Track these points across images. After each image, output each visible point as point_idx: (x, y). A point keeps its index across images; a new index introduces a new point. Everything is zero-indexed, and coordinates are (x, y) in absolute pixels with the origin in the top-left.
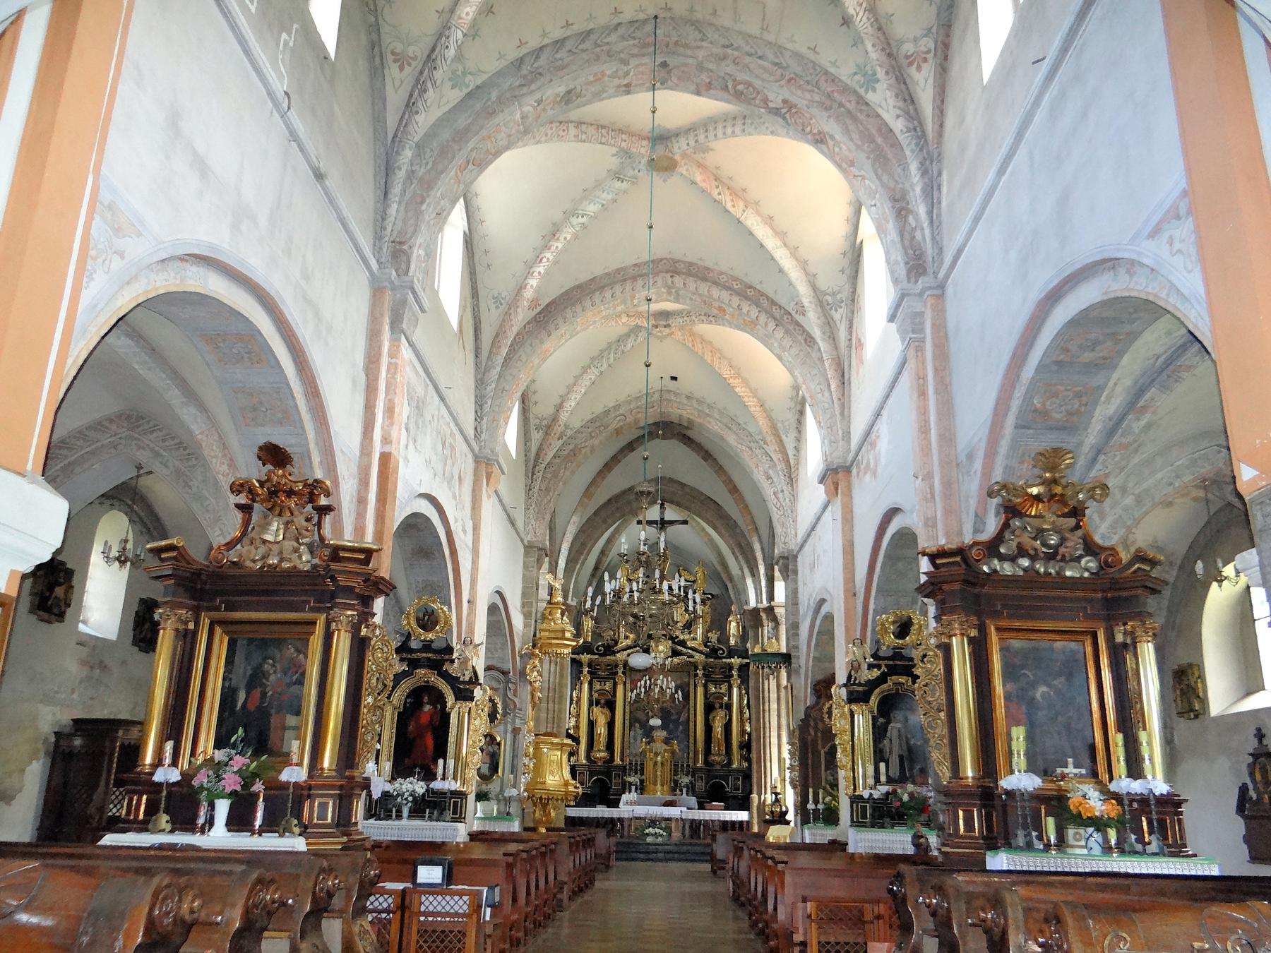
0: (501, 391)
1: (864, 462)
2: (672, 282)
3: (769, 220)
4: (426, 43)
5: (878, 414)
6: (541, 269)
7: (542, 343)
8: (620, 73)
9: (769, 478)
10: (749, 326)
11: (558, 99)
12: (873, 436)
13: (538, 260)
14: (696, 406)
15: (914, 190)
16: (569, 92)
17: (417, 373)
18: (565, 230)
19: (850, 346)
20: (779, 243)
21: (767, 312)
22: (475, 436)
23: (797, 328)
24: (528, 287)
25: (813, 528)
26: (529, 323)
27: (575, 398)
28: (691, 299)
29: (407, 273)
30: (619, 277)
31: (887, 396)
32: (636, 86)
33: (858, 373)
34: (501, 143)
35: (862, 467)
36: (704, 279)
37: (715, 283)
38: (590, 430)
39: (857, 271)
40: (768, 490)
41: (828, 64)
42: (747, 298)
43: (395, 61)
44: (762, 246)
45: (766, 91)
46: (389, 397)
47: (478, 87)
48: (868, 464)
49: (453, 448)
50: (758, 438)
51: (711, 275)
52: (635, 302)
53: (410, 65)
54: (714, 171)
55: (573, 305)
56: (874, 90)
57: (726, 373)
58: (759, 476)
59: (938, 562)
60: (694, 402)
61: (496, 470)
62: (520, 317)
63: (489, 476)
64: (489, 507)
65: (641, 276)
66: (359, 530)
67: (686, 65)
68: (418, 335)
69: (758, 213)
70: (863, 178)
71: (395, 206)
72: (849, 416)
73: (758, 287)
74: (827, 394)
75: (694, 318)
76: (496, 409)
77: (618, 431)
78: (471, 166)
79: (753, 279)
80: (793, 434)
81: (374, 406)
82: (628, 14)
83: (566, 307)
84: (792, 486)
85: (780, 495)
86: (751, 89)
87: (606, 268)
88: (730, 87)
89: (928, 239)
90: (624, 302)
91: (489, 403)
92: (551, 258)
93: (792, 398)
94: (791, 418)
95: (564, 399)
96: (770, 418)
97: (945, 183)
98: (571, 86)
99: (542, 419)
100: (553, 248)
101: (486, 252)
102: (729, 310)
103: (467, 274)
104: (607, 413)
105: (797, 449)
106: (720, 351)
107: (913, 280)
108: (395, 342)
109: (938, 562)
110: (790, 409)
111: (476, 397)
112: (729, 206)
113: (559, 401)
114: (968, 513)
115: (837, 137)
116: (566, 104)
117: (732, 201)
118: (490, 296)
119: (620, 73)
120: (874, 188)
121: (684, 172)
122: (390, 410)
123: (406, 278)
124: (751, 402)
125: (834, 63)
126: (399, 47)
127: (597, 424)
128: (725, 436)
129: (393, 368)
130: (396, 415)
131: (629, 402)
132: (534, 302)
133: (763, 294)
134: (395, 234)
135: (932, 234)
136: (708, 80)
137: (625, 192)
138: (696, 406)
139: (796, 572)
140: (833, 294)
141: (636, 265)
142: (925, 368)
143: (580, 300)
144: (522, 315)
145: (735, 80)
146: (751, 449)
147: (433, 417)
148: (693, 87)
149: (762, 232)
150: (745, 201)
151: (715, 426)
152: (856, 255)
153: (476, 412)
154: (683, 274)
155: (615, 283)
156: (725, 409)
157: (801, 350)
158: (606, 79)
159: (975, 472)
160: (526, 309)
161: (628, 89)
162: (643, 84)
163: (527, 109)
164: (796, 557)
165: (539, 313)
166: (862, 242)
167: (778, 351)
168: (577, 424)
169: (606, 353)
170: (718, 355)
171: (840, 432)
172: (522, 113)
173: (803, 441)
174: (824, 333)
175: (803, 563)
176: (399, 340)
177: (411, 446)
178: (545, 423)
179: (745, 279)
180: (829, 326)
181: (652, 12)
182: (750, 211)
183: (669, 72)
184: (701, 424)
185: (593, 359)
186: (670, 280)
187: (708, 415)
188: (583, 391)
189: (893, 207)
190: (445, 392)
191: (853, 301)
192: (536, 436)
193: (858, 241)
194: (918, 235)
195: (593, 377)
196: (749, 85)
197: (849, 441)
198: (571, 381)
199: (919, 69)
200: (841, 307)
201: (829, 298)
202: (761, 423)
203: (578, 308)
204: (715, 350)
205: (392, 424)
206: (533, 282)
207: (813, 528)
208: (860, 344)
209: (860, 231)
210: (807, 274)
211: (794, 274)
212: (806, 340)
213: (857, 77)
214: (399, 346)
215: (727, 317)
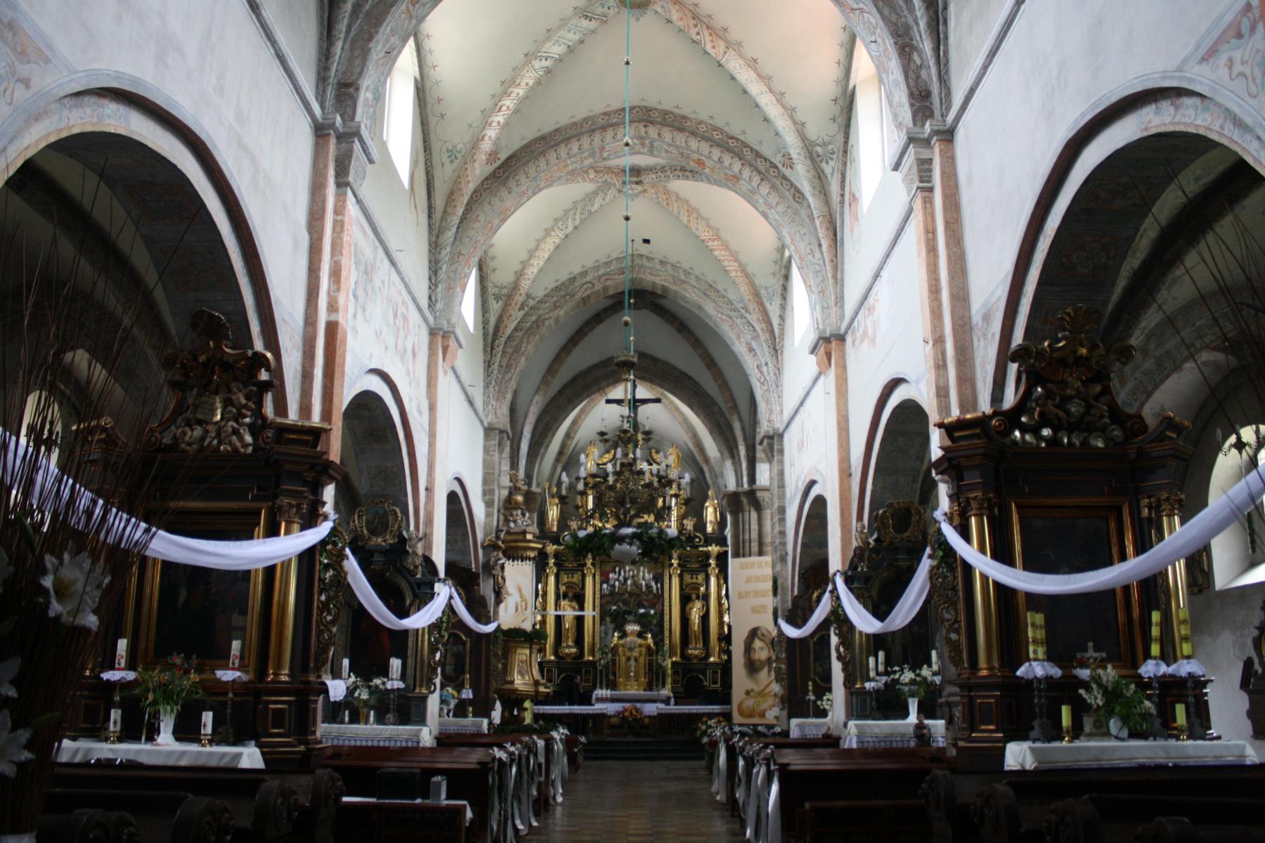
0: (456, 256)
1: (861, 330)
2: (646, 132)
3: (753, 63)
5: (877, 276)
6: (500, 118)
7: (501, 200)
9: (751, 350)
10: (731, 181)
12: (871, 300)
13: (495, 107)
14: (671, 272)
15: (917, 24)
17: (365, 233)
18: (528, 75)
19: (842, 202)
20: (764, 88)
21: (751, 165)
22: (430, 306)
23: (785, 182)
24: (486, 138)
25: (802, 404)
26: (487, 179)
27: (537, 263)
28: (667, 151)
29: (353, 118)
30: (586, 127)
31: (888, 256)
33: (852, 231)
35: (858, 335)
36: (681, 130)
37: (693, 134)
38: (554, 299)
39: (849, 119)
40: (750, 364)
42: (729, 150)
44: (745, 92)
46: (334, 259)
48: (865, 332)
49: (405, 319)
50: (739, 306)
51: (689, 124)
52: (605, 155)
54: (692, 8)
55: (536, 158)
57: (705, 235)
58: (740, 349)
59: (957, 434)
60: (669, 267)
61: (452, 344)
62: (477, 172)
63: (445, 349)
64: (446, 383)
65: (612, 125)
66: (305, 409)
68: (365, 190)
69: (741, 56)
70: (862, 11)
71: (340, 44)
72: (842, 280)
73: (741, 137)
74: (818, 255)
75: (669, 173)
76: (452, 275)
77: (585, 300)
79: (735, 130)
80: (778, 301)
81: (319, 269)
83: (528, 162)
84: (777, 358)
85: (764, 369)
87: (572, 117)
89: (935, 79)
90: (592, 155)
91: (444, 268)
92: (512, 106)
93: (776, 262)
94: (776, 284)
95: (525, 264)
96: (752, 284)
97: (953, 17)
99: (502, 287)
100: (513, 95)
101: (439, 100)
102: (709, 163)
103: (419, 123)
104: (572, 280)
105: (782, 318)
106: (697, 210)
107: (919, 123)
108: (341, 198)
109: (957, 434)
110: (774, 274)
111: (430, 262)
112: (709, 48)
113: (518, 267)
114: (985, 383)
117: (712, 41)
118: (444, 149)
120: (873, 21)
121: (659, 10)
122: (336, 274)
123: (352, 124)
124: (732, 266)
127: (562, 293)
128: (703, 305)
129: (339, 226)
130: (343, 279)
131: (597, 268)
132: (493, 155)
133: (746, 146)
134: (339, 74)
135: (940, 74)
137: (593, 32)
138: (671, 272)
139: (781, 452)
140: (824, 144)
141: (605, 114)
142: (933, 221)
143: (543, 153)
144: (479, 170)
146: (730, 317)
147: (383, 282)
149: (746, 77)
150: (726, 42)
151: (691, 295)
152: (848, 100)
153: (430, 279)
154: (658, 123)
155: (582, 134)
156: (703, 275)
157: (789, 207)
159: (993, 335)
160: (484, 162)
164: (781, 436)
165: (499, 168)
166: (854, 87)
167: (763, 208)
168: (540, 293)
169: (571, 213)
170: (695, 215)
171: (833, 298)
173: (788, 308)
174: (814, 188)
175: (790, 442)
176: (345, 194)
177: (359, 315)
178: (505, 291)
179: (726, 129)
180: (820, 179)
182: (731, 52)
184: (676, 292)
185: (556, 220)
186: (643, 130)
187: (684, 282)
188: (546, 256)
189: (896, 43)
190: (396, 256)
191: (845, 152)
192: (495, 307)
193: (851, 87)
194: (923, 74)
195: (557, 241)
197: (842, 307)
198: (532, 245)
200: (832, 159)
201: (819, 149)
202: (743, 289)
203: (542, 162)
204: (691, 210)
205: (338, 289)
206: (492, 133)
207: (802, 404)
208: (854, 198)
209: (853, 75)
210: (795, 123)
211: (781, 122)
212: (794, 196)
214: (345, 201)
215: (707, 171)
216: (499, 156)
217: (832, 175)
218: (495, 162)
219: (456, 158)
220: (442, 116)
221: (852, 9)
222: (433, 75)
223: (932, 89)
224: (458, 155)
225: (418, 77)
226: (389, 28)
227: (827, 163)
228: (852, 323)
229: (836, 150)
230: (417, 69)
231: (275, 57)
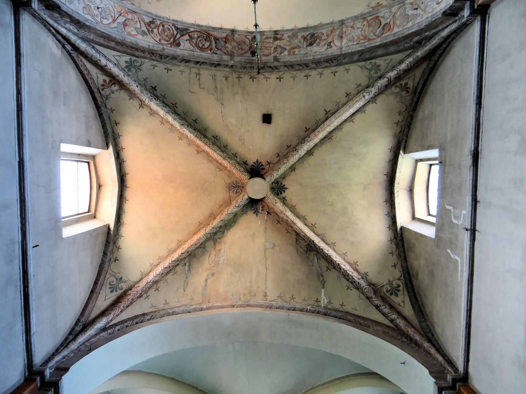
4: (389, 91)
8: (279, 50)
11: (318, 40)
16: (311, 44)
32: (270, 38)
34: (359, 25)
41: (157, 65)
43: (409, 88)
45: (192, 48)
47: (365, 61)
53: (401, 85)
56: (126, 62)
67: (241, 55)
70: (114, 21)
78: (383, 23)
82: (273, 76)
86: (201, 45)
88: (214, 42)
98: (309, 48)
115: (140, 37)
116: (314, 35)
120: (105, 22)
125: (155, 66)
126: (404, 93)
136: (228, 45)
145: (211, 49)
148: (236, 36)
158: (288, 48)
161: (276, 35)
162: (266, 38)
163: (337, 43)
172: (342, 42)
181: (261, 77)
183: (251, 47)
196: (202, 49)
199: (105, 81)
213: (138, 64)
221: (120, 15)
223: (47, 12)
226: (410, 24)
231: (482, 105)
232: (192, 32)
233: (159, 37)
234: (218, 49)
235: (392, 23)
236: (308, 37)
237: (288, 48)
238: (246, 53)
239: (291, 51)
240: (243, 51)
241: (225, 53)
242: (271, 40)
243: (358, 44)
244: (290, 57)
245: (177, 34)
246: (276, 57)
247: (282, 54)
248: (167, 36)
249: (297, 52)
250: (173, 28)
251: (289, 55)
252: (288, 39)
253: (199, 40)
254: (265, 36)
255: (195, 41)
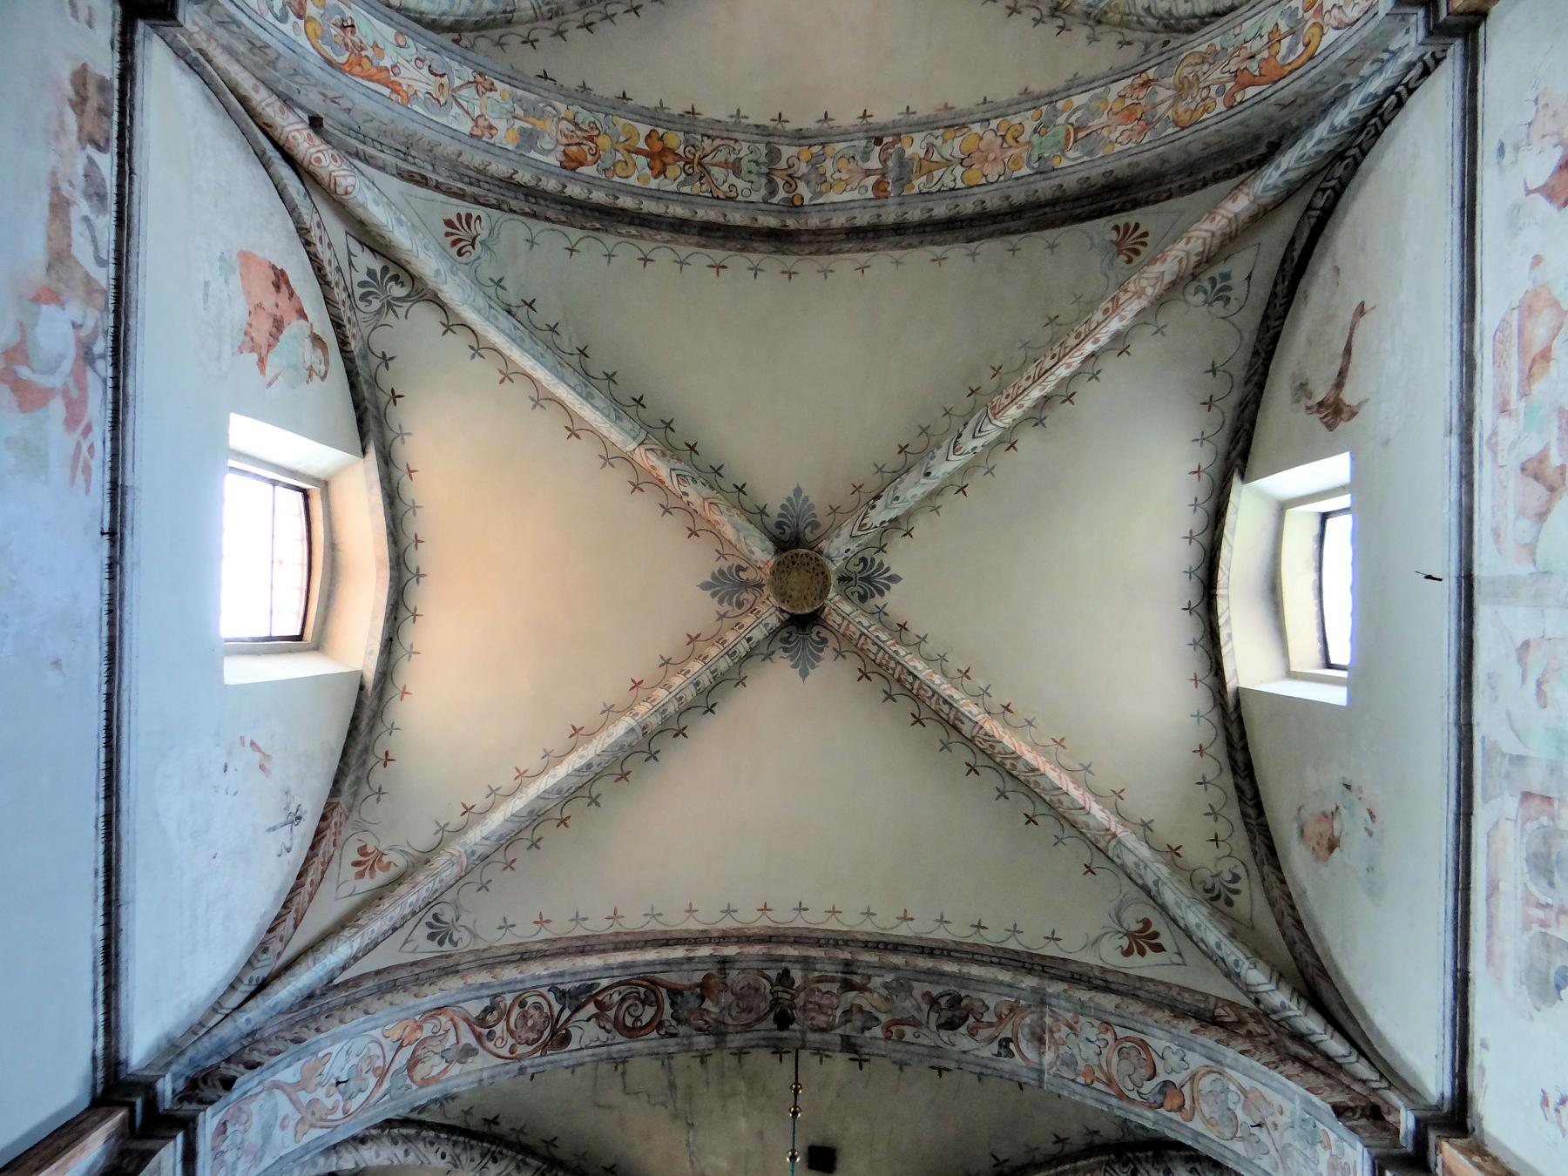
8: (858, 1021)
11: (971, 1020)
16: (951, 1025)
32: (832, 980)
45: (603, 1036)
67: (747, 1027)
86: (629, 1022)
98: (945, 1034)
101: (1209, 404)
115: (456, 1069)
116: (960, 999)
118: (1233, 306)
119: (858, 1021)
136: (708, 1004)
158: (884, 1018)
162: (820, 980)
172: (1042, 1054)
183: (776, 1002)
200: (362, 284)
201: (398, 291)
209: (375, 476)
216: (1114, 236)
217: (350, 253)
218: (1127, 226)
219: (1213, 281)
220: (1214, 371)
221: (401, 1046)
222: (1205, 457)
224: (1208, 287)
225: (1236, 480)
227: (371, 273)
228: (121, 167)
229: (361, 305)
230: (1233, 497)
232: (606, 989)
233: (511, 1041)
234: (679, 1021)
235: (1186, 1090)
236: (943, 1001)
237: (884, 1018)
238: (760, 1019)
239: (893, 1029)
240: (753, 1016)
241: (700, 1029)
242: (835, 988)
243: (1087, 1085)
244: (890, 1045)
245: (562, 1010)
246: (848, 1037)
247: (867, 1034)
248: (532, 1029)
249: (909, 1037)
250: (551, 996)
251: (888, 1038)
252: (884, 992)
253: (625, 1006)
254: (817, 974)
255: (611, 1013)
